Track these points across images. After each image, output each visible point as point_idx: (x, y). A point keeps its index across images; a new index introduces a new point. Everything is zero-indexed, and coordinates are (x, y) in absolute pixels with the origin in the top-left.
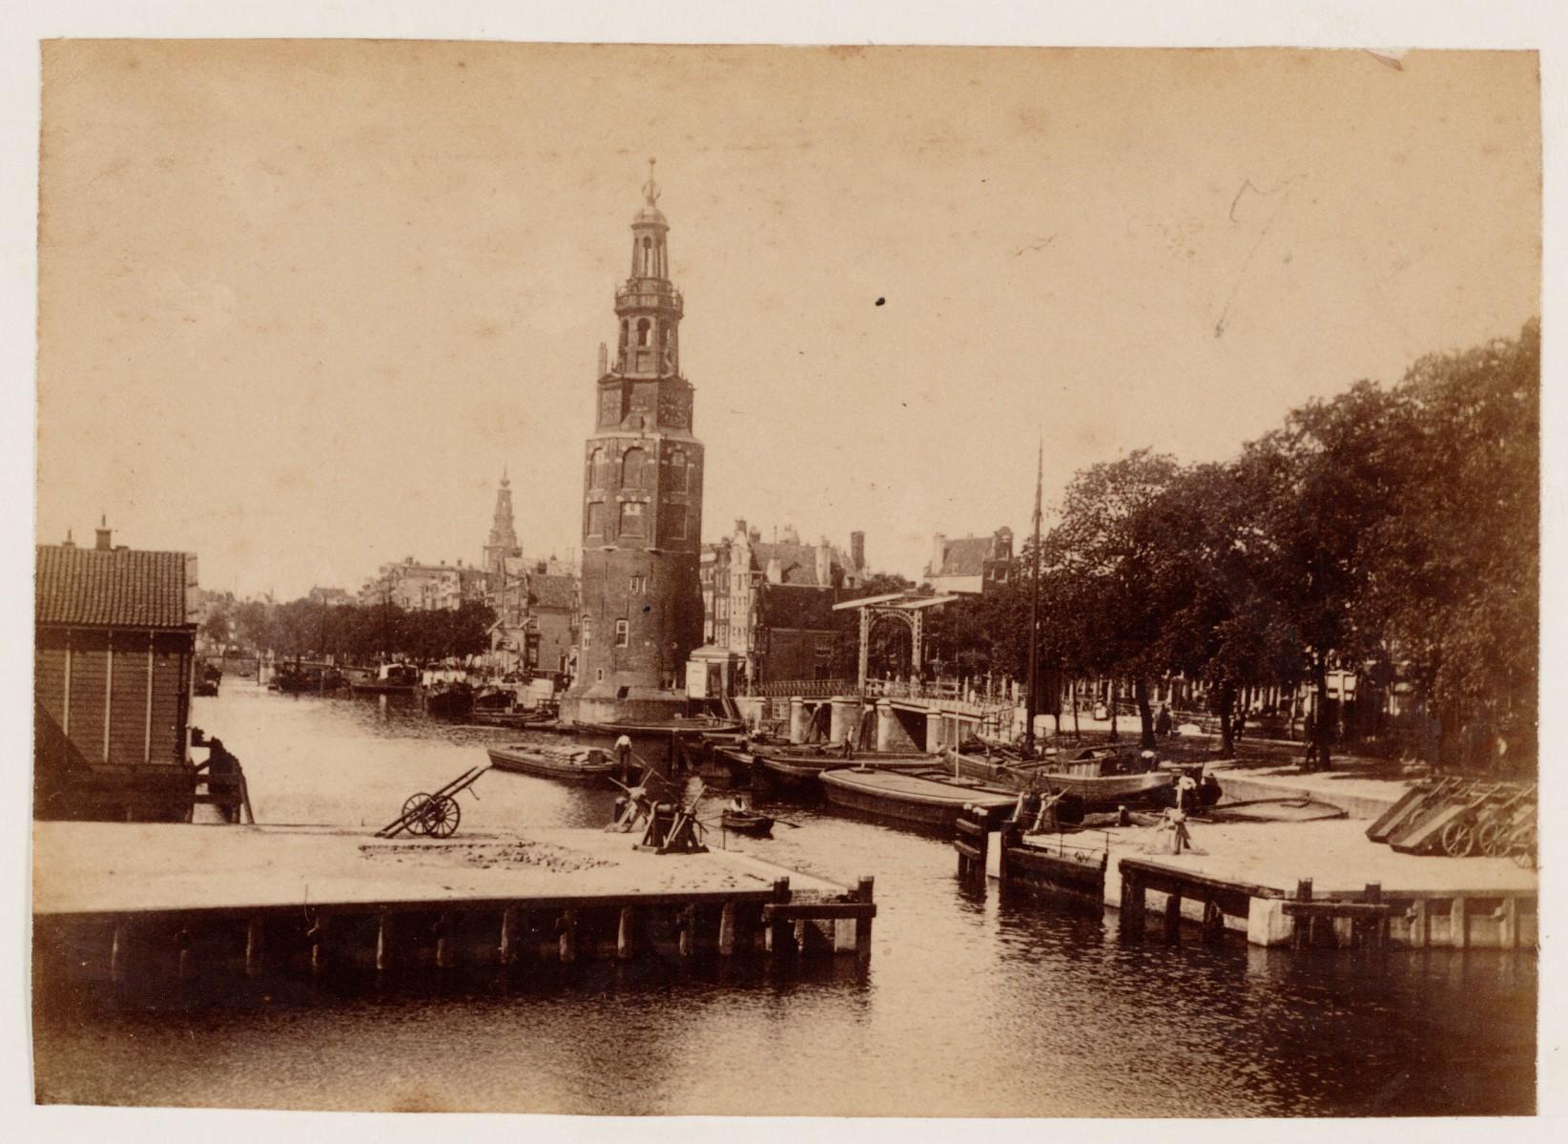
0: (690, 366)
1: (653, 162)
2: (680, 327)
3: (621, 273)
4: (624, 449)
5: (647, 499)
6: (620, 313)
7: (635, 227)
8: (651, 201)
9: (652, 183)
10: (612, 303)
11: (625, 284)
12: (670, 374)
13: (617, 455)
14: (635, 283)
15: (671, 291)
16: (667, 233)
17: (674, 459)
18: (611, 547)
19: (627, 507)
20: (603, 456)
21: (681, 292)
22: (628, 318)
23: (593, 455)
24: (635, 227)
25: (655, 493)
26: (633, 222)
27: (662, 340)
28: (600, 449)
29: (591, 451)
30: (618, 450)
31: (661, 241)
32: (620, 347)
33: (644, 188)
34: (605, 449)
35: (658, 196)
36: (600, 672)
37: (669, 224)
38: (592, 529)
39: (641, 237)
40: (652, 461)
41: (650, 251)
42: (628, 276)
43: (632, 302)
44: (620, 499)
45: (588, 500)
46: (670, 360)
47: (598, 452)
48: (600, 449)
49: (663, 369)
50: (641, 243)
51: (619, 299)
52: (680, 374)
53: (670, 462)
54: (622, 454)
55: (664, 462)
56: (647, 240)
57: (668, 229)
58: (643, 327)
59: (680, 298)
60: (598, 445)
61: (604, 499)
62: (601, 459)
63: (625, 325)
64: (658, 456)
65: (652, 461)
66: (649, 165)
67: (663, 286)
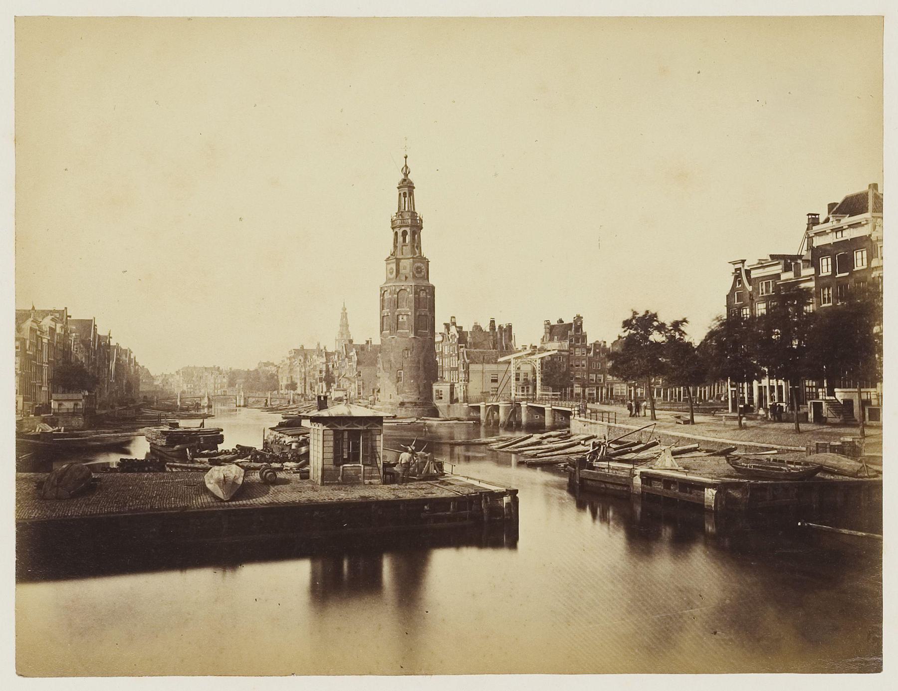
1: (406, 157)
4: (398, 290)
5: (410, 313)
13: (395, 294)
14: (400, 213)
18: (393, 337)
19: (400, 317)
20: (388, 294)
26: (398, 186)
27: (413, 239)
28: (386, 291)
29: (383, 292)
32: (394, 244)
34: (389, 291)
38: (385, 329)
45: (382, 315)
46: (417, 249)
48: (386, 291)
50: (402, 195)
51: (392, 222)
59: (421, 220)
61: (389, 314)
63: (396, 233)
64: (413, 293)
67: (413, 214)
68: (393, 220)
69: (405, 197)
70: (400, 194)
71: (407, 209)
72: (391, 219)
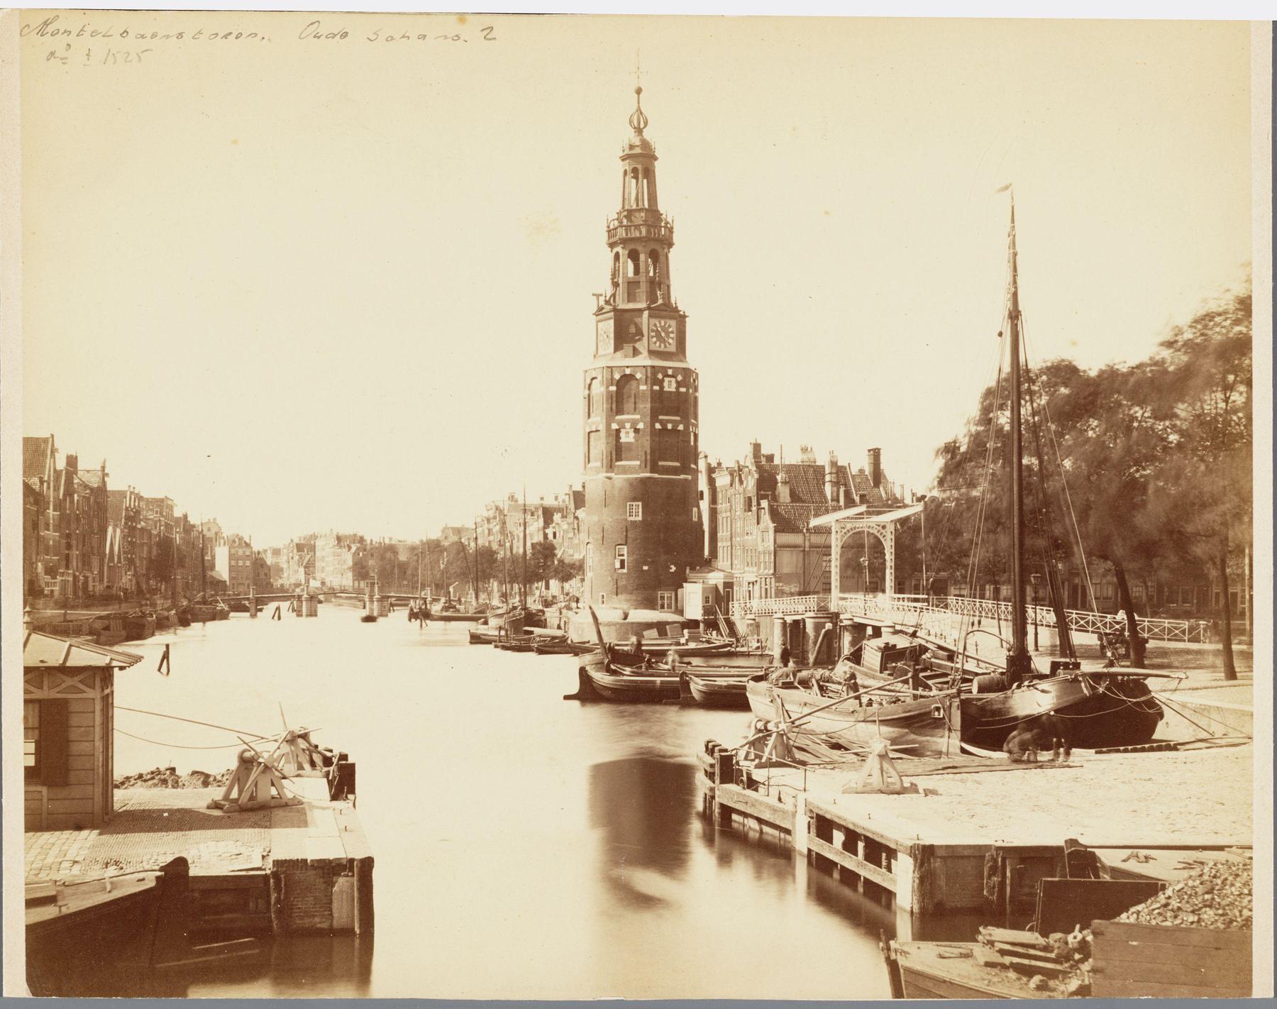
0: (681, 293)
1: (639, 91)
2: (670, 255)
3: (612, 208)
4: (617, 376)
5: (641, 426)
6: (612, 245)
10: (605, 235)
12: (660, 301)
13: (612, 385)
16: (656, 163)
17: (666, 384)
19: (622, 435)
21: (669, 220)
22: (619, 249)
23: (590, 385)
24: (623, 159)
25: (648, 419)
26: (622, 154)
29: (588, 381)
30: (612, 378)
31: (649, 173)
34: (600, 378)
36: (603, 596)
37: (657, 154)
40: (643, 388)
43: (621, 233)
44: (615, 426)
47: (594, 381)
48: (595, 378)
49: (652, 298)
50: (630, 175)
52: (673, 301)
53: (662, 387)
54: (615, 382)
55: (656, 388)
57: (656, 159)
58: (634, 256)
59: (671, 230)
62: (599, 389)
63: (617, 257)
65: (643, 388)
67: (653, 214)
68: (612, 227)
69: (636, 178)
70: (625, 172)
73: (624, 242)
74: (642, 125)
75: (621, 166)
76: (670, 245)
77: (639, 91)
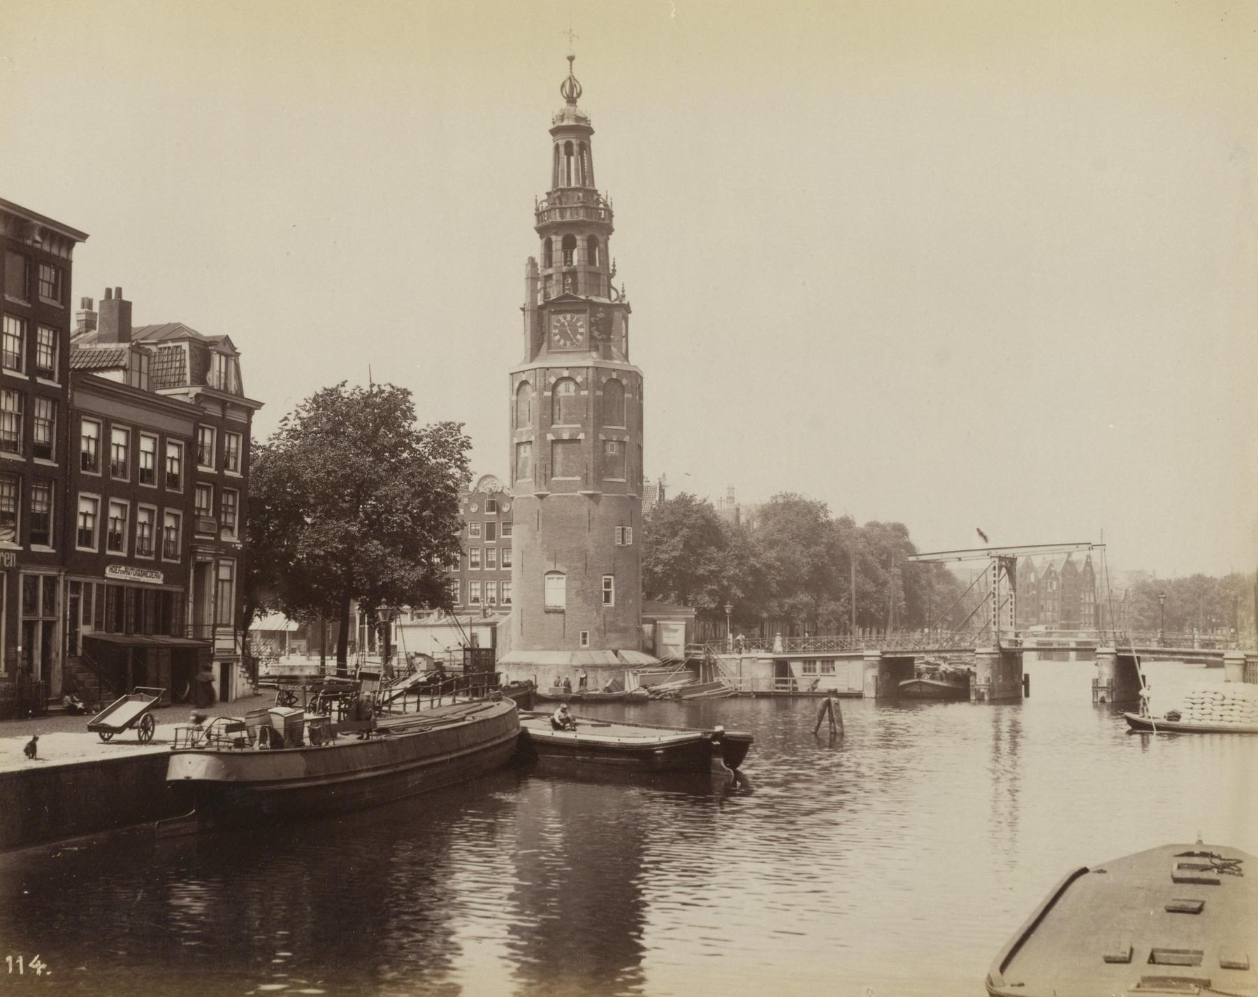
1: (571, 59)
2: (610, 243)
4: (553, 380)
6: (541, 231)
7: (554, 132)
8: (571, 100)
9: (572, 80)
10: (533, 221)
11: (545, 197)
13: (545, 389)
14: (558, 195)
15: (598, 201)
16: (592, 137)
24: (554, 132)
26: (552, 126)
29: (517, 385)
31: (585, 148)
33: (563, 86)
35: (579, 95)
39: (562, 142)
41: (572, 159)
42: (549, 187)
45: (516, 441)
50: (562, 149)
51: (539, 215)
56: (568, 146)
57: (591, 131)
58: (569, 245)
59: (610, 214)
60: (524, 377)
63: (548, 245)
64: (591, 386)
66: (568, 62)
67: (591, 193)
69: (569, 153)
70: (557, 148)
71: (573, 184)
72: (535, 206)
73: (557, 228)
74: (575, 95)
75: (548, 143)
76: (610, 230)
77: (571, 59)
